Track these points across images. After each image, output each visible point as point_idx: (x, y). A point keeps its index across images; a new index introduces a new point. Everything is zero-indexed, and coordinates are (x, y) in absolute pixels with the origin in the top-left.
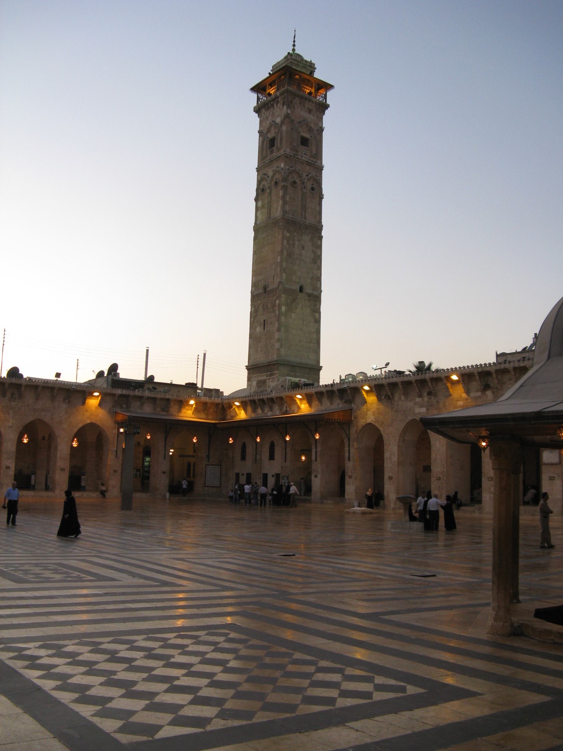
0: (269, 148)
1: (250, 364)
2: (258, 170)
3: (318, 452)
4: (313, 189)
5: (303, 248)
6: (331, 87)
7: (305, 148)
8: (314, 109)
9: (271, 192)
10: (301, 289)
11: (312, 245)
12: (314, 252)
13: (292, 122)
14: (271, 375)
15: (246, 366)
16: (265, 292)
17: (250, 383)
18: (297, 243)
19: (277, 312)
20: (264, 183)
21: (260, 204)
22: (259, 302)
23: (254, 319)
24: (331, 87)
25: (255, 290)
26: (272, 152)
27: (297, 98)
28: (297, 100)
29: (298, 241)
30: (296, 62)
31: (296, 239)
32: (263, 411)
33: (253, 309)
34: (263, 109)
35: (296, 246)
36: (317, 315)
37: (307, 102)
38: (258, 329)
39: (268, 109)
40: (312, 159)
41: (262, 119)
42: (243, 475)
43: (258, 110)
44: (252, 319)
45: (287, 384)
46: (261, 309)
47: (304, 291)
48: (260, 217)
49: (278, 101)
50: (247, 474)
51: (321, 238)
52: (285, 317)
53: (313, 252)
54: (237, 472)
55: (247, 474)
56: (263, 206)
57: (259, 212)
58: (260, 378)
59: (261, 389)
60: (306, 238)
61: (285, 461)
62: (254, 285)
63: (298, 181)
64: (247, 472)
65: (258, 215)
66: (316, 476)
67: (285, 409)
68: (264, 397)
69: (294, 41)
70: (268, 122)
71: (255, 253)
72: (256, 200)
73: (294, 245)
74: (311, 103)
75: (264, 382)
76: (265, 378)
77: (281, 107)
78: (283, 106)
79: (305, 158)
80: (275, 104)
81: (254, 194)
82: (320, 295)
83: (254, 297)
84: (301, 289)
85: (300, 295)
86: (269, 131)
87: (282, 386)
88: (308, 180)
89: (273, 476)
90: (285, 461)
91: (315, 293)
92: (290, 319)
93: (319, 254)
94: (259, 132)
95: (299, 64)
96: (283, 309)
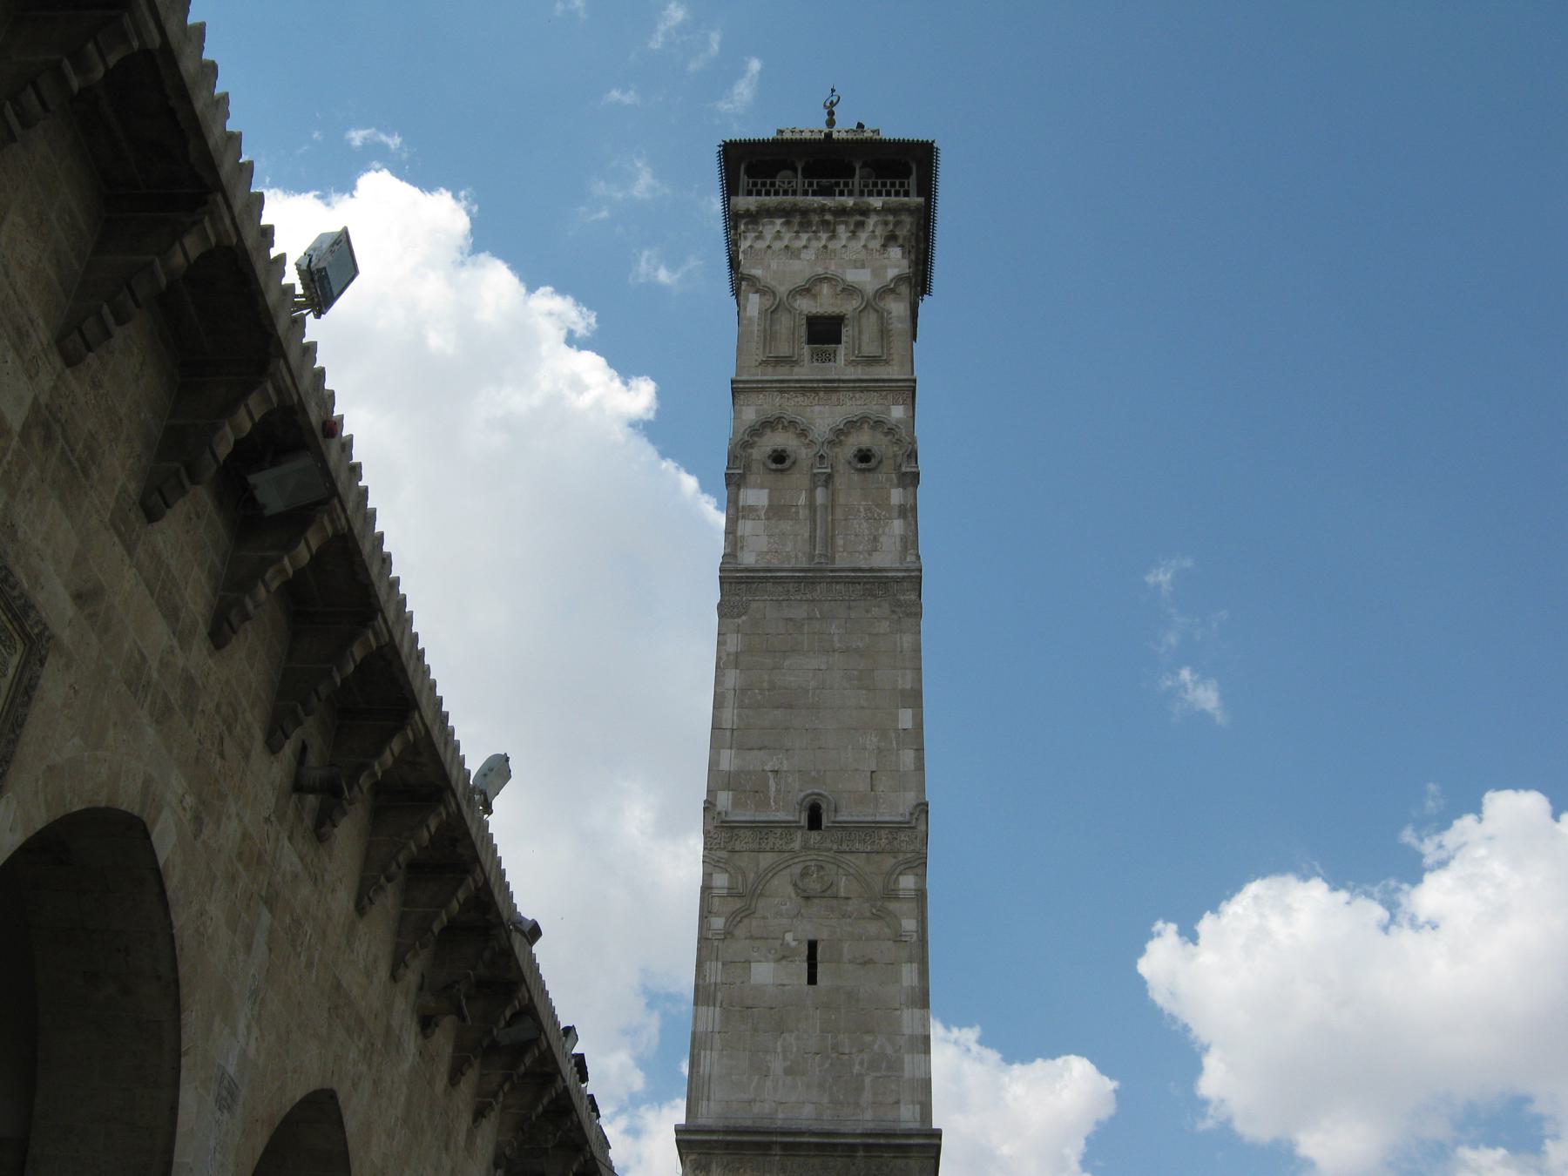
9: (830, 477)
22: (766, 860)
25: (736, 803)
26: (828, 358)
33: (721, 880)
34: (779, 221)
39: (805, 226)
44: (718, 923)
46: (782, 886)
49: (860, 225)
56: (777, 510)
77: (876, 244)
80: (841, 229)
86: (806, 291)
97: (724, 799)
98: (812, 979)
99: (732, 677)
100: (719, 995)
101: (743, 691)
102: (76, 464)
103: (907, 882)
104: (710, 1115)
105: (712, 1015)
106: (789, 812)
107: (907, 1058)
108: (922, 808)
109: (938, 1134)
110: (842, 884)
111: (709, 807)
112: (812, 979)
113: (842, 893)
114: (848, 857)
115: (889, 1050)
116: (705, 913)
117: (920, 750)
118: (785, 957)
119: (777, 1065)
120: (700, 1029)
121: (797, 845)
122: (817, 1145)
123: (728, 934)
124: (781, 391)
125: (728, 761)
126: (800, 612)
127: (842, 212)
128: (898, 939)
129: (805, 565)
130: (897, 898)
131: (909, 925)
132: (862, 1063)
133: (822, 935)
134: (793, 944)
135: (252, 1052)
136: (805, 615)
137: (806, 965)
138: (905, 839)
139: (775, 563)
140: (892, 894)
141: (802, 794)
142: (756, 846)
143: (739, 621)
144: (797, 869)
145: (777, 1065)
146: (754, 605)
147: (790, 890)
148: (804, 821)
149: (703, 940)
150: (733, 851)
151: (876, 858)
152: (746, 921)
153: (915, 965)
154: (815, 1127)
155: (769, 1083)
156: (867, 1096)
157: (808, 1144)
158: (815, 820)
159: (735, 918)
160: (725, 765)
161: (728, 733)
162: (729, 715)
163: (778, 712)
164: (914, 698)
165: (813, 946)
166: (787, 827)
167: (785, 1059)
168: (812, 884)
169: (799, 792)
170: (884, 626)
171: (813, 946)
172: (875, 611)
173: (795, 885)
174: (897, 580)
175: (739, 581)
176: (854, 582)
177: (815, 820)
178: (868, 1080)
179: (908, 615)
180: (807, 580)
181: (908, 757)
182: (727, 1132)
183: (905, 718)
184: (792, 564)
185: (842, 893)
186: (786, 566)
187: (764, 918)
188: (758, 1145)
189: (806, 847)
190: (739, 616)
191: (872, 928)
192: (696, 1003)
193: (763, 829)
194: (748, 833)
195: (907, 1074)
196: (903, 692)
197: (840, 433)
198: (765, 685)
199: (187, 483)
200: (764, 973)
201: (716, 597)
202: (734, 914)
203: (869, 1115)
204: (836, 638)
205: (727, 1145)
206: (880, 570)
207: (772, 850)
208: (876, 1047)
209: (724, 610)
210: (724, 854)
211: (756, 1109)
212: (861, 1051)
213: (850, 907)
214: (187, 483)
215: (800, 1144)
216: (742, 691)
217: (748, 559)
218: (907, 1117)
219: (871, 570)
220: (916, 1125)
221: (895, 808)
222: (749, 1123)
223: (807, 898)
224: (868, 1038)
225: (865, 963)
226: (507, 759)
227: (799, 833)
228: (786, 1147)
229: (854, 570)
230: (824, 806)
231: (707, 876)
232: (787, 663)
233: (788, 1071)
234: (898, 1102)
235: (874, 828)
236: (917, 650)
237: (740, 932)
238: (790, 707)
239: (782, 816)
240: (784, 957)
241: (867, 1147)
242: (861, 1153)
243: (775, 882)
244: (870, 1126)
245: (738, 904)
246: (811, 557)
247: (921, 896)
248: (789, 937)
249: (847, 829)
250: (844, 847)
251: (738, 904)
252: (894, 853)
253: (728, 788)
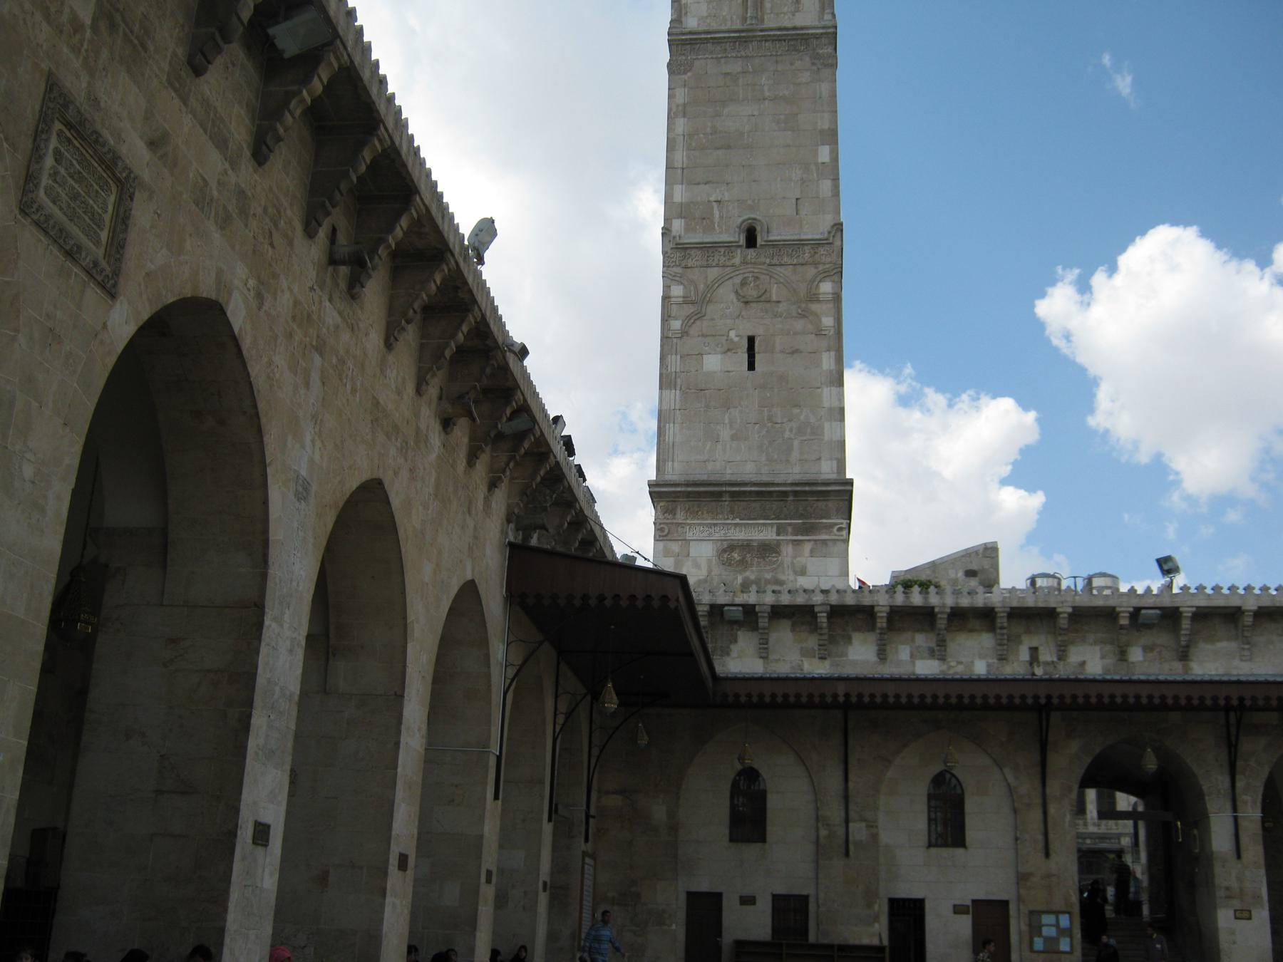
3: (1243, 824)
14: (808, 529)
15: (651, 485)
17: (675, 547)
22: (713, 273)
25: (688, 228)
32: (882, 655)
33: (677, 291)
42: (748, 900)
44: (676, 325)
46: (726, 293)
50: (776, 898)
54: (704, 886)
55: (776, 898)
58: (740, 535)
59: (751, 574)
61: (1047, 855)
64: (781, 890)
66: (1243, 914)
68: (934, 600)
75: (767, 550)
76: (769, 535)
89: (958, 910)
90: (1047, 855)
97: (678, 225)
98: (751, 366)
99: (681, 124)
100: (679, 381)
101: (691, 136)
102: (136, 42)
103: (826, 287)
104: (675, 473)
105: (674, 396)
106: (732, 234)
107: (827, 425)
108: (838, 227)
109: (850, 482)
110: (774, 291)
111: (666, 232)
112: (751, 366)
113: (774, 298)
114: (779, 268)
115: (812, 420)
116: (666, 318)
117: (836, 180)
118: (729, 349)
119: (725, 433)
120: (665, 407)
121: (737, 260)
122: (758, 493)
123: (684, 333)
125: (679, 195)
126: (735, 67)
128: (819, 333)
129: (739, 27)
130: (818, 301)
131: (828, 321)
132: (791, 430)
133: (758, 331)
134: (736, 339)
135: (317, 457)
136: (739, 69)
137: (746, 356)
138: (825, 253)
139: (714, 26)
140: (813, 297)
141: (741, 220)
142: (705, 263)
143: (685, 77)
144: (738, 280)
145: (725, 433)
146: (697, 63)
147: (733, 297)
148: (742, 241)
149: (665, 338)
150: (686, 267)
151: (800, 269)
152: (698, 323)
153: (833, 353)
154: (755, 479)
155: (719, 446)
156: (795, 455)
157: (751, 492)
158: (751, 240)
159: (690, 320)
160: (678, 198)
161: (679, 171)
162: (680, 156)
163: (720, 152)
164: (831, 136)
165: (751, 340)
166: (729, 247)
167: (731, 427)
168: (751, 292)
169: (738, 217)
170: (805, 77)
171: (751, 340)
172: (798, 64)
173: (737, 292)
174: (817, 37)
175: (684, 43)
176: (779, 39)
177: (751, 240)
178: (796, 443)
179: (825, 66)
180: (741, 40)
181: (826, 185)
182: (688, 485)
183: (824, 154)
184: (728, 26)
185: (774, 298)
186: (723, 28)
187: (713, 319)
188: (712, 494)
189: (744, 262)
190: (685, 73)
191: (799, 325)
192: (661, 388)
193: (709, 248)
194: (699, 252)
195: (826, 438)
196: (822, 132)
198: (708, 130)
199: (221, 43)
200: (713, 362)
201: (666, 57)
202: (689, 317)
203: (797, 469)
204: (766, 88)
205: (688, 494)
206: (802, 28)
207: (717, 266)
208: (802, 417)
209: (672, 68)
210: (679, 270)
211: (710, 466)
212: (790, 421)
213: (781, 308)
214: (221, 43)
215: (744, 492)
217: (692, 23)
218: (826, 470)
219: (795, 28)
220: (833, 476)
221: (815, 228)
222: (705, 478)
223: (746, 303)
224: (796, 411)
225: (793, 353)
226: (493, 222)
227: (739, 251)
228: (733, 494)
229: (780, 29)
230: (758, 228)
231: (666, 288)
232: (726, 111)
233: (734, 438)
234: (819, 459)
235: (799, 244)
236: (833, 95)
237: (694, 331)
238: (729, 147)
239: (725, 238)
240: (729, 350)
241: (796, 493)
242: (791, 498)
243: (721, 290)
244: (797, 478)
245: (690, 309)
246: (744, 19)
247: (837, 299)
248: (732, 334)
249: (775, 245)
250: (775, 261)
251: (690, 309)
252: (816, 264)
253: (680, 216)
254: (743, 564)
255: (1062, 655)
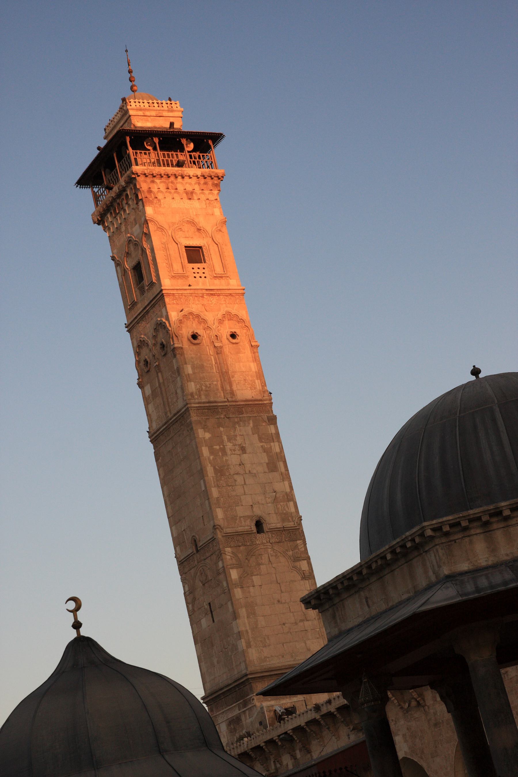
0: (137, 285)
1: (208, 692)
2: (130, 328)
4: (233, 336)
5: (243, 450)
6: (217, 138)
7: (198, 265)
8: (197, 188)
10: (259, 525)
11: (260, 439)
12: (267, 451)
13: (161, 228)
14: (245, 704)
16: (197, 551)
18: (229, 446)
19: (225, 584)
20: (145, 353)
21: (148, 389)
22: (192, 571)
23: (193, 606)
24: (217, 138)
25: (181, 551)
27: (158, 181)
28: (159, 185)
29: (229, 440)
30: (141, 113)
31: (225, 438)
33: (187, 589)
35: (229, 452)
36: (304, 565)
37: (179, 179)
38: (205, 622)
40: (217, 281)
41: (111, 234)
43: (100, 220)
44: (190, 606)
45: (268, 716)
47: (265, 528)
48: (154, 417)
51: (273, 420)
52: (242, 588)
53: (265, 450)
56: (153, 392)
57: (150, 406)
58: (231, 715)
60: (245, 431)
62: (178, 542)
63: (200, 331)
65: (150, 412)
67: (273, 767)
69: (130, 72)
70: (123, 238)
71: (164, 482)
72: (141, 385)
73: (223, 451)
74: (187, 179)
76: (236, 712)
77: (135, 206)
78: (137, 204)
79: (204, 284)
81: (135, 375)
82: (300, 524)
83: (184, 564)
84: (259, 525)
85: (261, 538)
86: (128, 254)
87: (261, 723)
88: (221, 322)
91: (291, 524)
92: (251, 589)
93: (278, 450)
94: (113, 258)
95: (148, 113)
96: (234, 574)
119: (215, 660)
124: (138, 323)
127: (119, 195)
176: (176, 421)
185: (210, 579)
197: (155, 337)
216: (169, 496)
219: (178, 412)
233: (218, 663)
239: (190, 551)
250: (205, 557)
254: (235, 730)
255: (281, 764)
